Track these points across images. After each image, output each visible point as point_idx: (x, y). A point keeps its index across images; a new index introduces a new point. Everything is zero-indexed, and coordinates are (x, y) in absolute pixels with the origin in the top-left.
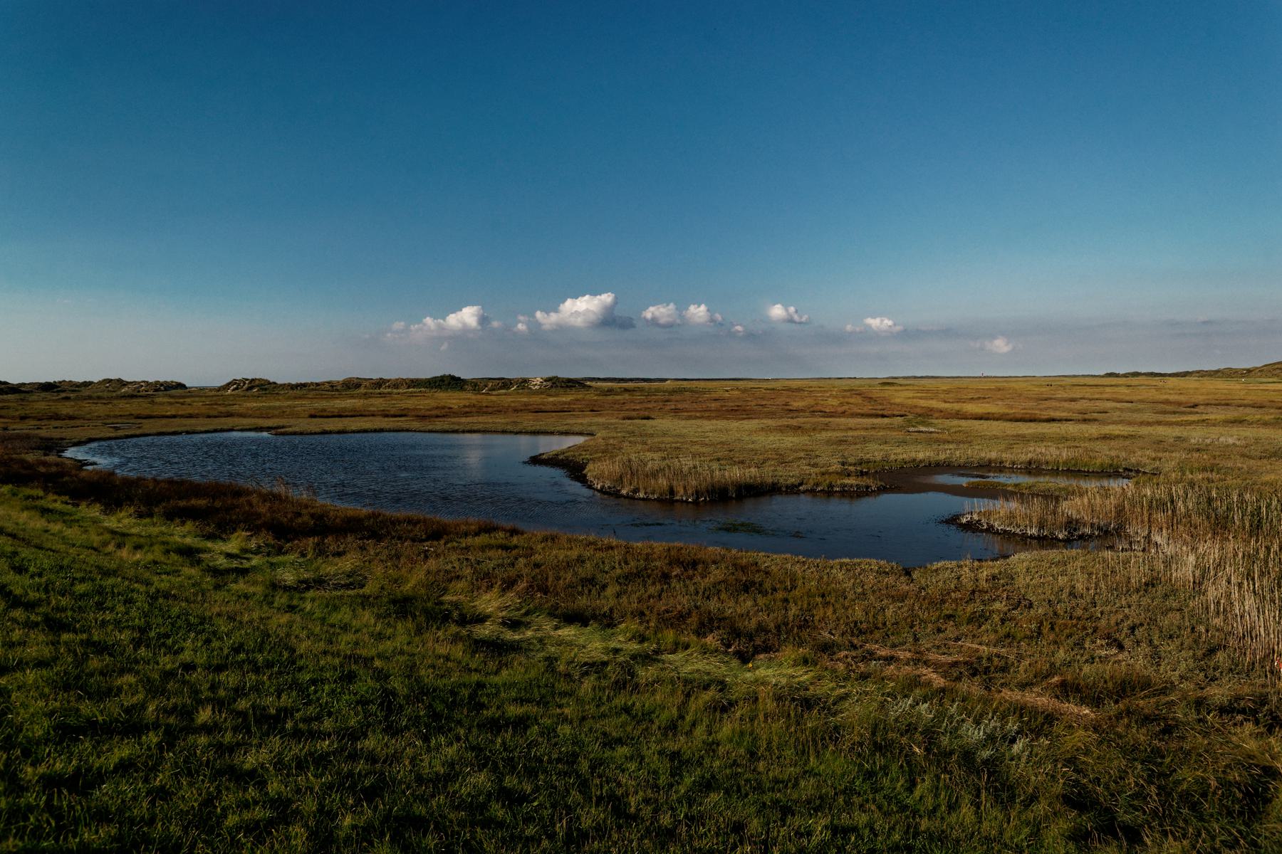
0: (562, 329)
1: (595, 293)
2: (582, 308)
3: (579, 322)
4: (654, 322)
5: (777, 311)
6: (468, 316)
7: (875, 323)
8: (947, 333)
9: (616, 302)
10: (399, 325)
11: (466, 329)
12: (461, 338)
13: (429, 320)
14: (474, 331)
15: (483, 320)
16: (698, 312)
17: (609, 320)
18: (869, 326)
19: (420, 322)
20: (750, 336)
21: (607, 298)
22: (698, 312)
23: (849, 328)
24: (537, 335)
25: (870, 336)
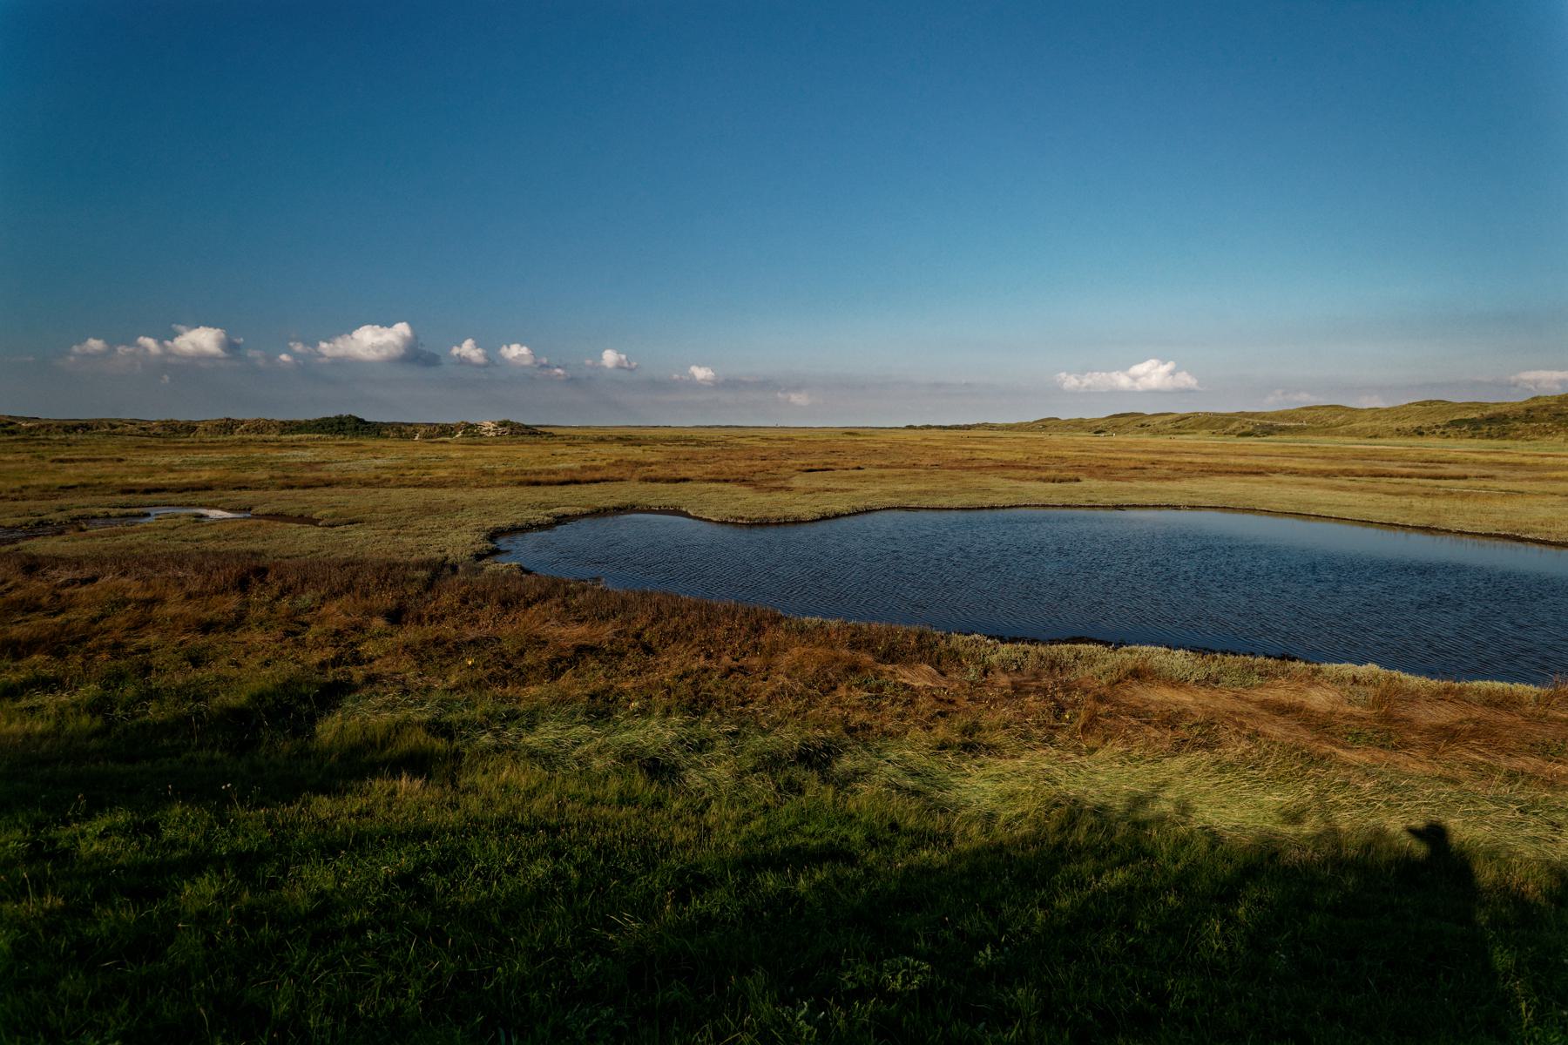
0: (342, 363)
1: (390, 324)
2: (373, 341)
3: (372, 355)
4: (464, 361)
5: (609, 357)
6: (202, 340)
7: (701, 373)
8: (766, 385)
9: (415, 336)
10: (95, 344)
11: (202, 357)
12: (193, 368)
13: (149, 343)
14: (213, 358)
15: (230, 346)
16: (515, 351)
17: (415, 356)
18: (693, 376)
19: (130, 341)
20: (572, 381)
21: (402, 328)
22: (515, 351)
23: (676, 376)
24: (310, 370)
25: (694, 385)
